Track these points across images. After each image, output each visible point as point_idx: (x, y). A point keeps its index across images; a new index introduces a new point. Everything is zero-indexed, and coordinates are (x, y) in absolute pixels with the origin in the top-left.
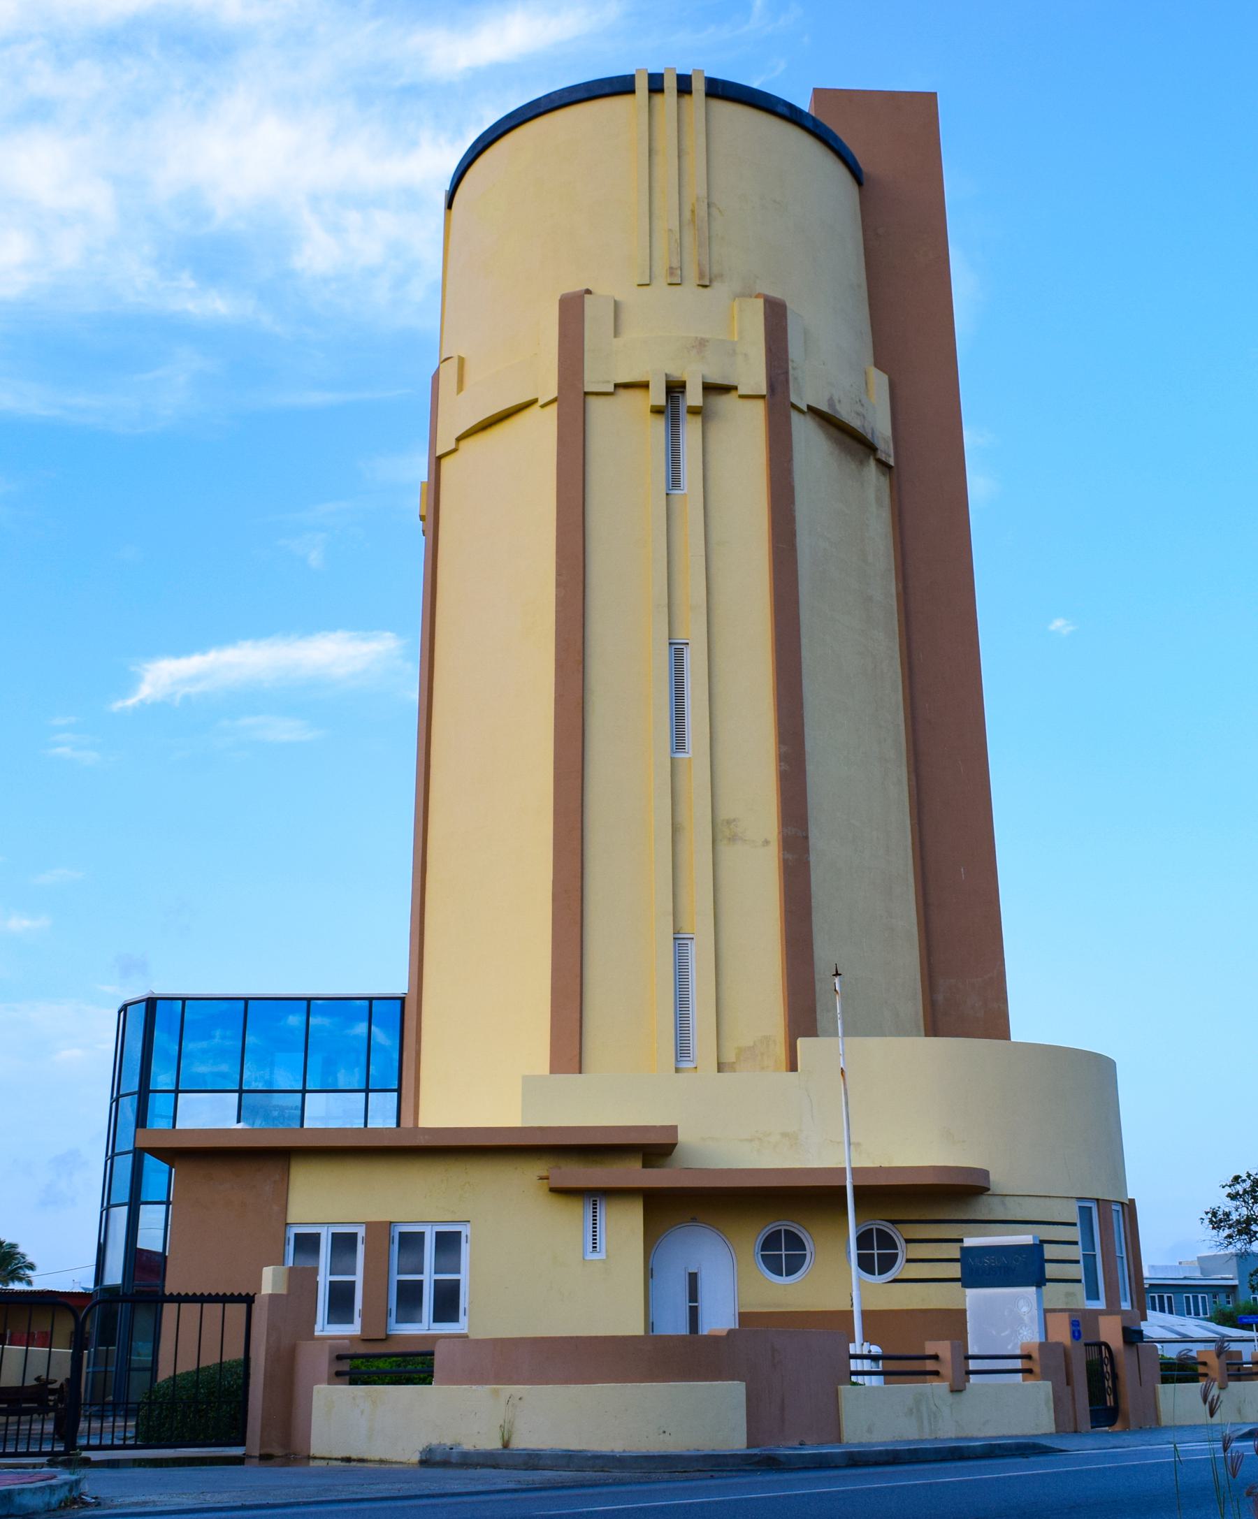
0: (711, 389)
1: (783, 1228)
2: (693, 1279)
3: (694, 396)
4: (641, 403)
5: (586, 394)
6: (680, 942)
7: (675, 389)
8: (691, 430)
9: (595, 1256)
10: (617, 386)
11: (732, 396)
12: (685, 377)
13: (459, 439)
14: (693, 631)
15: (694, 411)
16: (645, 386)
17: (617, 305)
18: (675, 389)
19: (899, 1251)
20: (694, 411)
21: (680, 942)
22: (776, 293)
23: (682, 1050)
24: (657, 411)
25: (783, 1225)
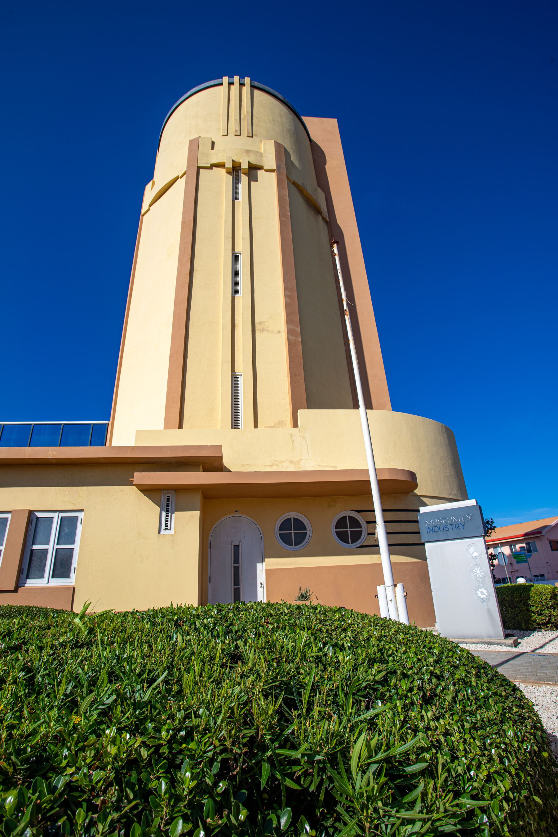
1: (292, 517)
2: (236, 549)
3: (245, 166)
5: (199, 168)
6: (235, 379)
8: (244, 179)
9: (168, 532)
12: (241, 161)
13: (150, 206)
14: (242, 247)
19: (363, 529)
21: (235, 379)
23: (235, 424)
25: (292, 515)
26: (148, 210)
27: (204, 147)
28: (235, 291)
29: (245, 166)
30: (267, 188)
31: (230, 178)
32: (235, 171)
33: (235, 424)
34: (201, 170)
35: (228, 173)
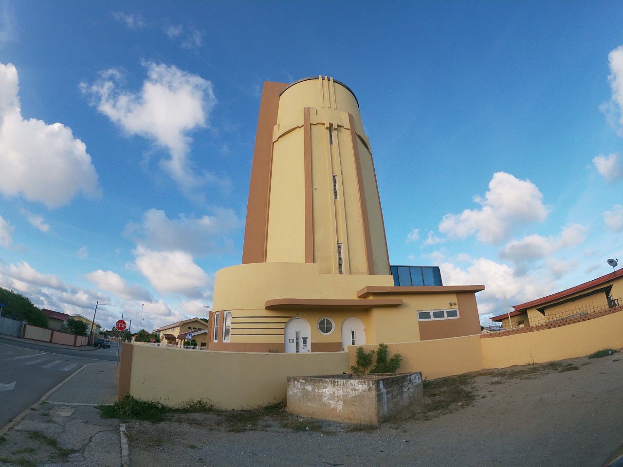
0: (339, 126)
3: (335, 126)
4: (323, 128)
7: (331, 125)
10: (317, 123)
11: (342, 129)
13: (278, 138)
14: (337, 172)
15: (335, 129)
16: (324, 124)
17: (317, 110)
18: (331, 125)
20: (335, 129)
22: (350, 113)
23: (340, 272)
24: (327, 128)
26: (277, 140)
27: (313, 113)
28: (336, 197)
29: (335, 126)
30: (346, 137)
31: (328, 131)
32: (330, 128)
33: (340, 272)
34: (313, 126)
35: (327, 128)
